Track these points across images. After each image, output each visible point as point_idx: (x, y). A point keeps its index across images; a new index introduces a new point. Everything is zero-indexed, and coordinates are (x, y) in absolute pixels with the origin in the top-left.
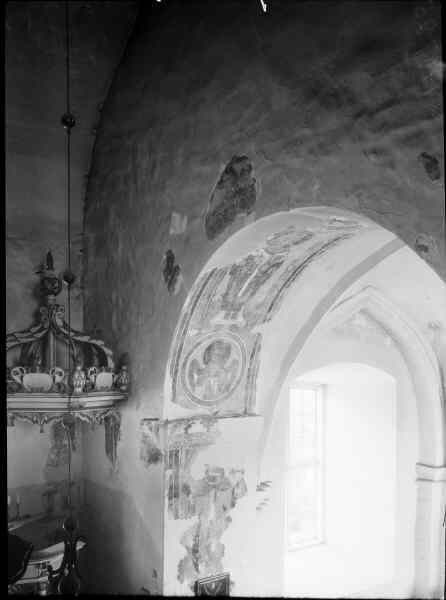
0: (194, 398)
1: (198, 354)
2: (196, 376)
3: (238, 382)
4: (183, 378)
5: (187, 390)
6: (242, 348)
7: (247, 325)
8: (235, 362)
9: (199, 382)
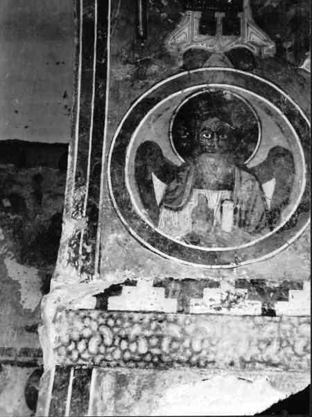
1: (151, 129)
2: (159, 187)
4: (119, 189)
5: (131, 216)
6: (291, 115)
7: (280, 50)
8: (276, 153)
9: (173, 201)
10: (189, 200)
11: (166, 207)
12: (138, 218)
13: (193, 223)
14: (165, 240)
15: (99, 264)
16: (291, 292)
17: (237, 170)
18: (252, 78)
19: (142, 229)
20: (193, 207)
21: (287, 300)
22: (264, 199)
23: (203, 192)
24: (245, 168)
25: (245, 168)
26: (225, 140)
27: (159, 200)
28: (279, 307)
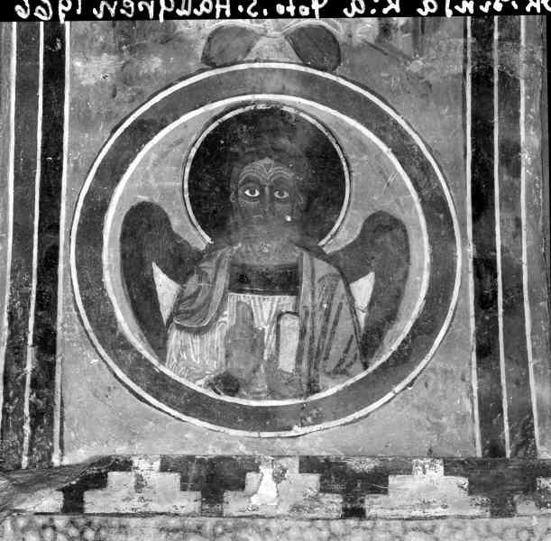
0: (162, 387)
2: (166, 288)
3: (425, 329)
5: (117, 346)
6: (405, 151)
9: (193, 315)
10: (219, 313)
11: (180, 328)
12: (128, 347)
13: (227, 356)
14: (178, 387)
15: (61, 433)
16: (392, 480)
17: (306, 257)
18: (335, 84)
19: (138, 368)
20: (227, 327)
21: (386, 492)
22: (353, 312)
23: (246, 298)
24: (320, 254)
25: (320, 254)
26: (285, 201)
27: (165, 314)
28: (373, 505)
